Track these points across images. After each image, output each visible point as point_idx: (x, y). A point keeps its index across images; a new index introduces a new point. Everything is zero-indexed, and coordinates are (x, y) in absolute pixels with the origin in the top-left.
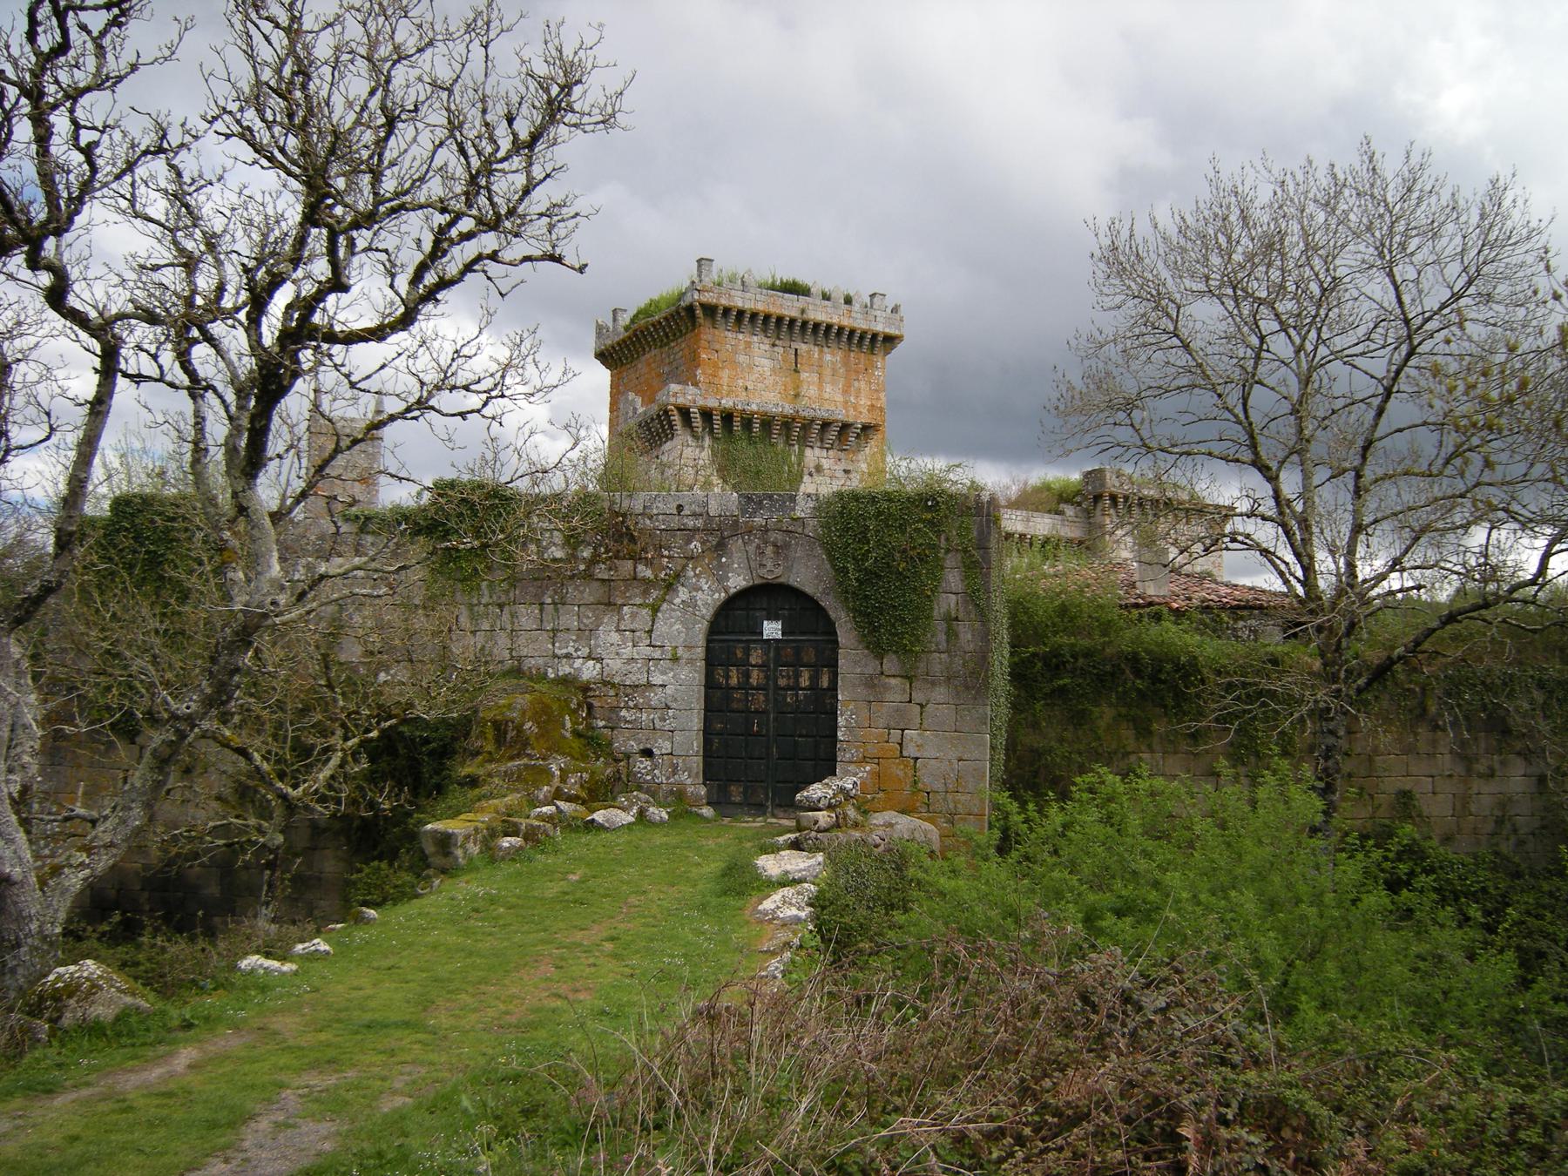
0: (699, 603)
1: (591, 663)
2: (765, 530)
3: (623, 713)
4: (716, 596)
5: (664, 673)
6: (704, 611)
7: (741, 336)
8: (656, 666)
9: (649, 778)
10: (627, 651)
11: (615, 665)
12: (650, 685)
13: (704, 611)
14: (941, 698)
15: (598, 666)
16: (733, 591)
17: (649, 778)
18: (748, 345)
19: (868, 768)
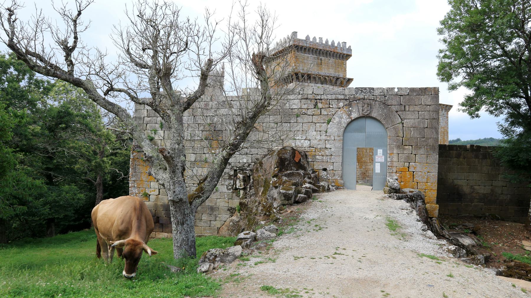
0: (342, 122)
1: (307, 141)
2: (364, 99)
3: (317, 157)
4: (348, 120)
5: (331, 144)
6: (344, 125)
7: (306, 55)
8: (328, 142)
9: (326, 177)
10: (318, 137)
11: (314, 142)
12: (325, 148)
13: (344, 125)
14: (422, 153)
15: (309, 142)
16: (353, 118)
17: (326, 177)
18: (308, 57)
19: (398, 175)
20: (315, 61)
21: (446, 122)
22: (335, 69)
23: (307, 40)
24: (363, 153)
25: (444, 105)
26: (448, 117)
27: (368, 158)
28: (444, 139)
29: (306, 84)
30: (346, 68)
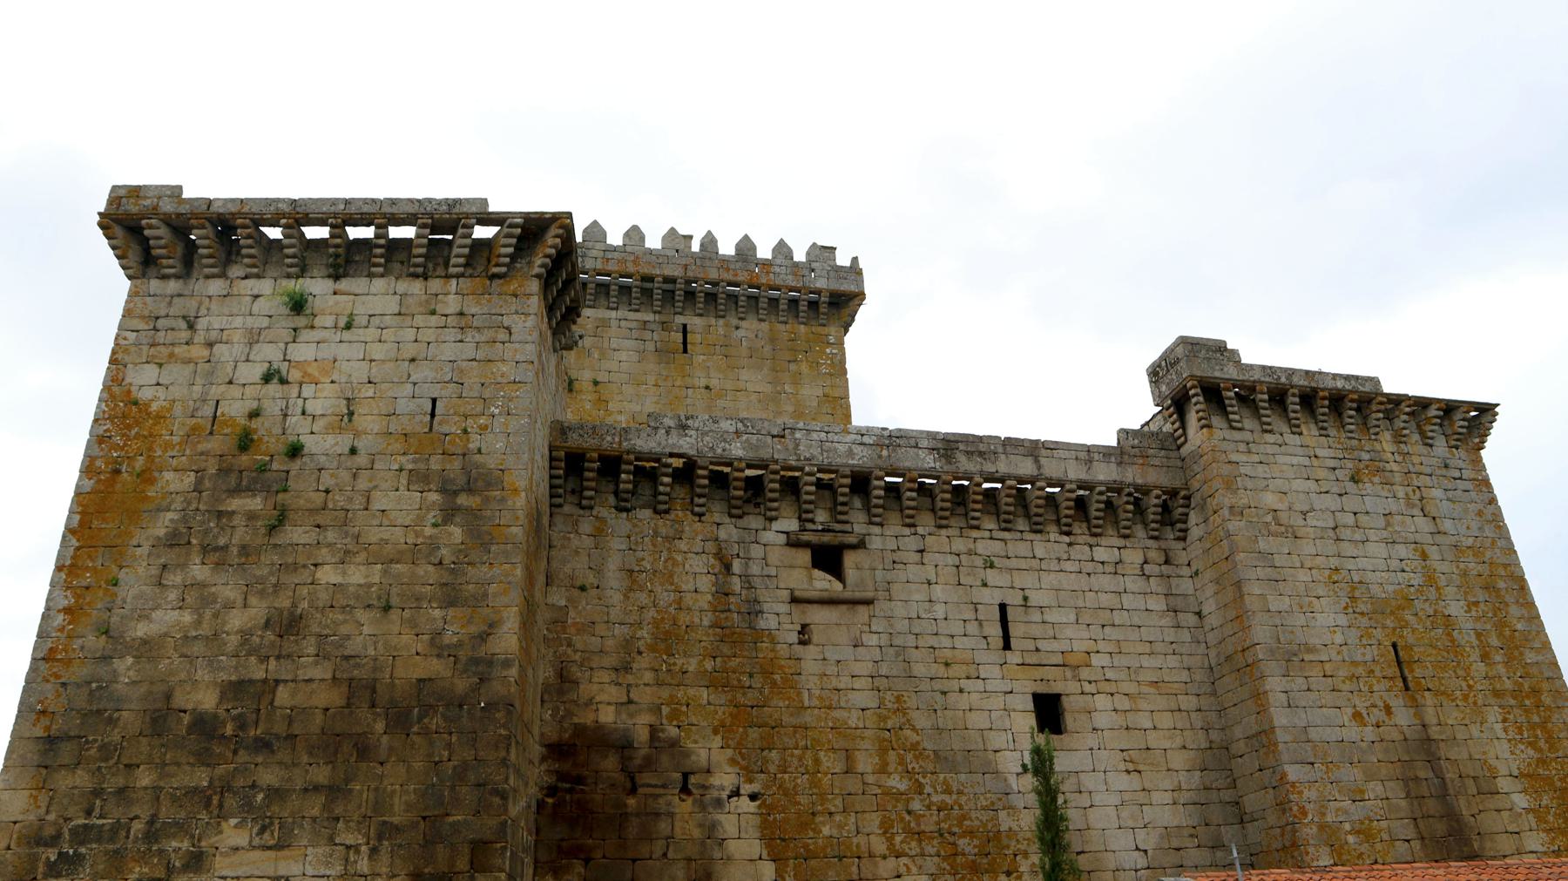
20: (648, 335)
21: (1480, 513)
22: (774, 370)
23: (590, 244)
24: (815, 784)
25: (1423, 404)
26: (1486, 482)
27: (873, 822)
28: (1501, 625)
29: (216, 287)
30: (843, 361)
